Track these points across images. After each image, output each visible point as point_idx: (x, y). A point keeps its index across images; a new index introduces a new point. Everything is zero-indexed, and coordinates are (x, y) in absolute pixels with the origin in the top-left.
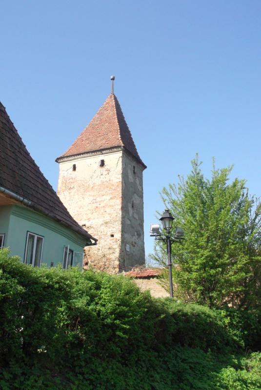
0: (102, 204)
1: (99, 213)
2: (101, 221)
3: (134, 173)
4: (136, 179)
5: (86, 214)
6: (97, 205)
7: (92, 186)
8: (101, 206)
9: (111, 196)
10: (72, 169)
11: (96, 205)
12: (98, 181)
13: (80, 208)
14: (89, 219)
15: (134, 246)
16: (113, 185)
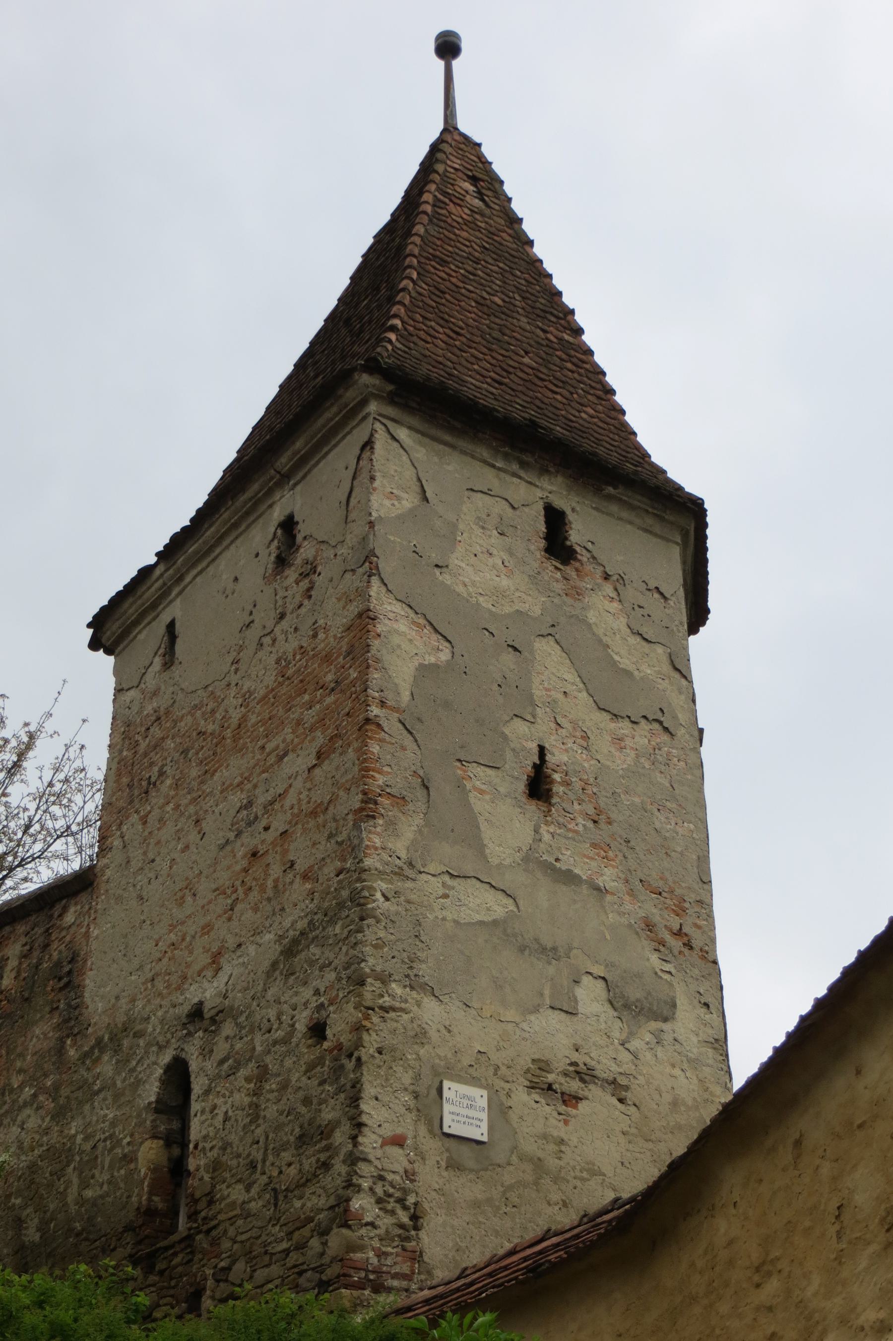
0: (279, 824)
1: (263, 888)
2: (265, 948)
3: (557, 544)
4: (577, 594)
5: (207, 928)
6: (249, 841)
7: (235, 716)
8: (270, 836)
9: (320, 738)
10: (158, 661)
11: (249, 841)
12: (261, 675)
13: (181, 902)
14: (216, 958)
15: (571, 1099)
16: (327, 659)
